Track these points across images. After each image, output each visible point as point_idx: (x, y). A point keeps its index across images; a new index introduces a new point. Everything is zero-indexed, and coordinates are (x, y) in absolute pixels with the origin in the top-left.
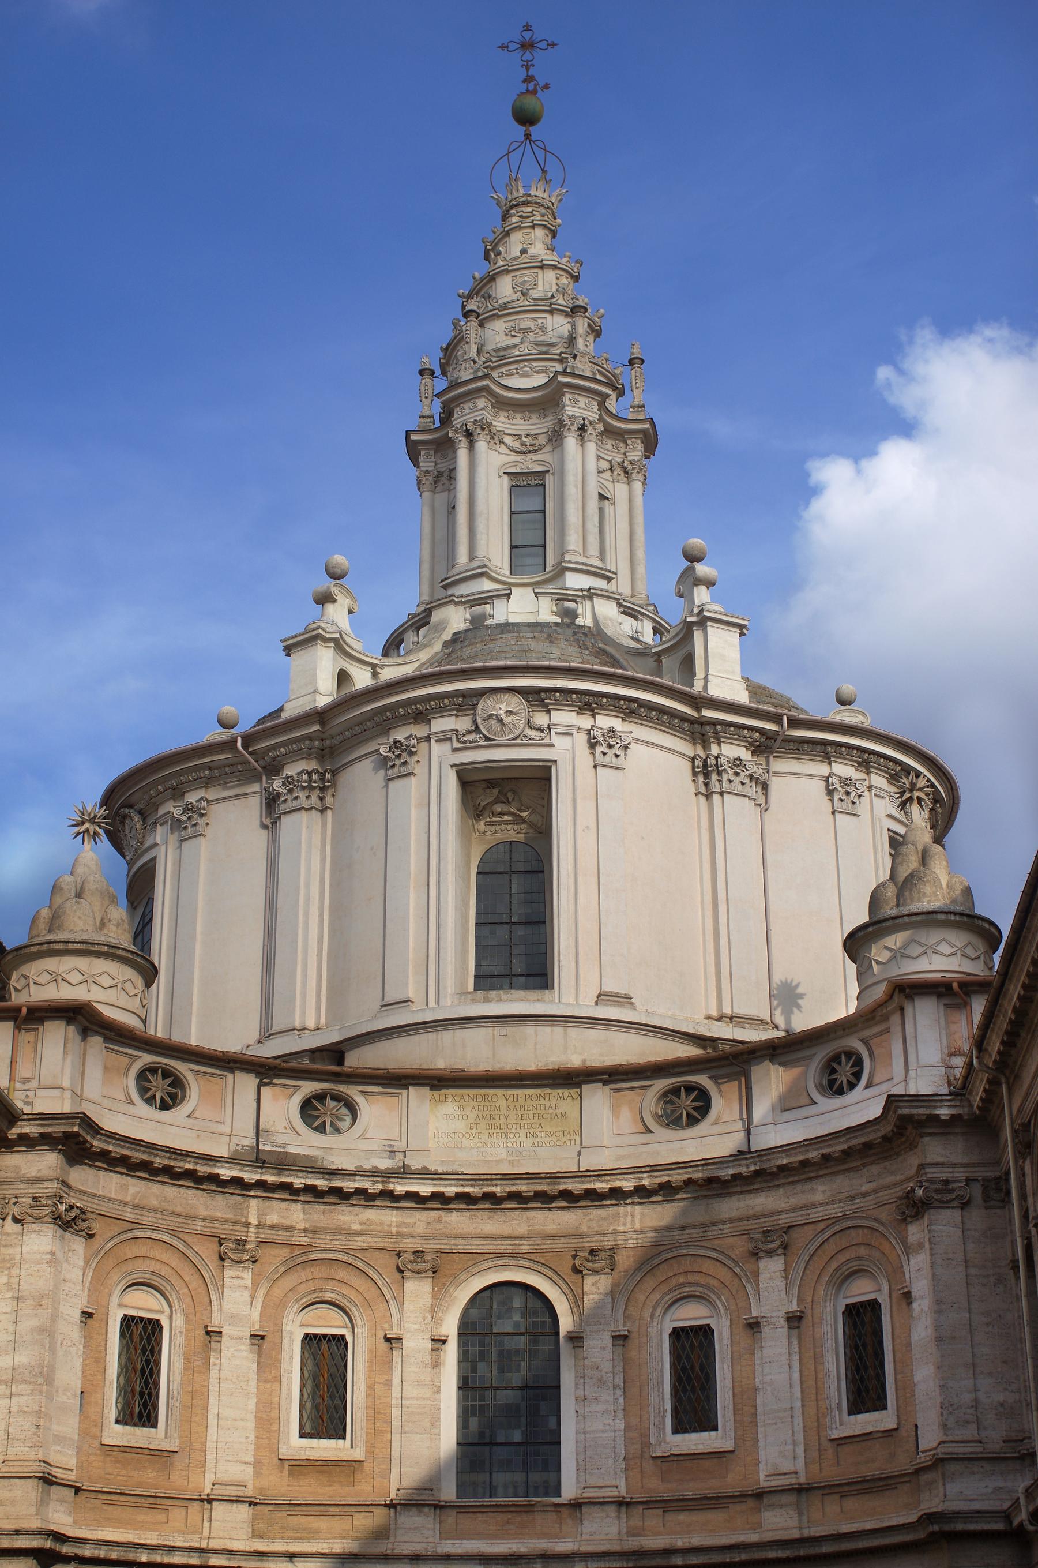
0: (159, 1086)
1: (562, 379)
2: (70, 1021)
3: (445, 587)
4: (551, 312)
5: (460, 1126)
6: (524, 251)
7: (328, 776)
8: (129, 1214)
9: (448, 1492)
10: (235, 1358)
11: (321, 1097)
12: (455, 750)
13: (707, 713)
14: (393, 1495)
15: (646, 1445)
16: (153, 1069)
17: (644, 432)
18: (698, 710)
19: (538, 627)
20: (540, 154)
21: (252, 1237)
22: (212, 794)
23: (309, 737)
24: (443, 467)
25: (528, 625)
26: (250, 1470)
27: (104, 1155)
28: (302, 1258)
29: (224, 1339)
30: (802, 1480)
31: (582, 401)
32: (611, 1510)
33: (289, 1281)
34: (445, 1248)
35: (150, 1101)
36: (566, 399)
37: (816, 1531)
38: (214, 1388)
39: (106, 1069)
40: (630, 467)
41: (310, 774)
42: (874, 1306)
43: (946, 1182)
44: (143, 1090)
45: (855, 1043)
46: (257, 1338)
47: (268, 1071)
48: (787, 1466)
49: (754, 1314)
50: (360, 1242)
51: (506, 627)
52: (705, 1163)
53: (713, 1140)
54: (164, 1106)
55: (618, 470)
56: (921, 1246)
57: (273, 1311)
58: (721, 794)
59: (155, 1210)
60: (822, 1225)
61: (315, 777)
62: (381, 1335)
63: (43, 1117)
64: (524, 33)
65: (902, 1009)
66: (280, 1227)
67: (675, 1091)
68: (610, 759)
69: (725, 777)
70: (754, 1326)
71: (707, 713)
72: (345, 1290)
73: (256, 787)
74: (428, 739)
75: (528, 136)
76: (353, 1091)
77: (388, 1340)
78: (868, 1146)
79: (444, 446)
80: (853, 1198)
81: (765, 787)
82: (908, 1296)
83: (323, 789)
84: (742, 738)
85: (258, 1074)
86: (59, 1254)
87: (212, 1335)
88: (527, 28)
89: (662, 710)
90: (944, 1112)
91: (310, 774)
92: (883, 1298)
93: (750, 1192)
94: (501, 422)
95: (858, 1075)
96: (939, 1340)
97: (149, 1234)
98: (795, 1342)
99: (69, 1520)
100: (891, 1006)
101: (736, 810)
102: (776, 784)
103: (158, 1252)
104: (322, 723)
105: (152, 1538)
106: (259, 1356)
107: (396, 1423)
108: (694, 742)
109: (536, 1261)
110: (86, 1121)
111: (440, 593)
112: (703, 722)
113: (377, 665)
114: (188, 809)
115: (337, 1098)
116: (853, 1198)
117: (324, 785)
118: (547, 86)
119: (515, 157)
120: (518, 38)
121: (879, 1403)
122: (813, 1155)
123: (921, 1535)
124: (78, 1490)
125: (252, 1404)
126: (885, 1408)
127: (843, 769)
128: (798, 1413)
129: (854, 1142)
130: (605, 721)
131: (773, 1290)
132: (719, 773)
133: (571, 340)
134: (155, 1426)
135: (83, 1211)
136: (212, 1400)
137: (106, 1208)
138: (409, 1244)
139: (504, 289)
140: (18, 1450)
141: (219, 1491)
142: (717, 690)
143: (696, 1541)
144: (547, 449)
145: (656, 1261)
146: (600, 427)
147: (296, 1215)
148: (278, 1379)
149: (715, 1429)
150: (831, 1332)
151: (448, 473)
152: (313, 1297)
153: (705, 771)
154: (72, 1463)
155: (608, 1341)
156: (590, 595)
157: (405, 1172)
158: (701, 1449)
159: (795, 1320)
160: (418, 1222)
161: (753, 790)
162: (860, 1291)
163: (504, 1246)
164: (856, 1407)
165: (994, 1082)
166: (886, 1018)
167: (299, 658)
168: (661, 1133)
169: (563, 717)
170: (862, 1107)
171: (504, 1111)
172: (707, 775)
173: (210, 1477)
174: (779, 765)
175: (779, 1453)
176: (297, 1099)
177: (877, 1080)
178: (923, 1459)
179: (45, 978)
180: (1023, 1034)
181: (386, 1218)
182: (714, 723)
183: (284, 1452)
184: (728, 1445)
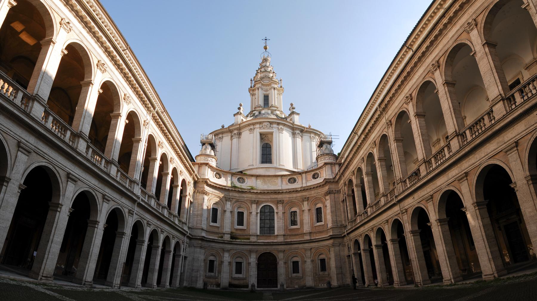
0: (218, 176)
5: (260, 183)
9: (259, 234)
10: (228, 214)
15: (287, 227)
28: (237, 201)
33: (236, 204)
45: (318, 172)
46: (231, 212)
47: (233, 174)
50: (246, 199)
53: (297, 186)
57: (233, 208)
67: (291, 178)
70: (303, 211)
73: (230, 134)
76: (244, 177)
78: (320, 186)
82: (326, 206)
87: (225, 211)
90: (332, 181)
94: (263, 87)
101: (299, 140)
109: (272, 202)
114: (220, 138)
117: (240, 134)
122: (312, 187)
130: (281, 126)
131: (306, 206)
143: (295, 240)
147: (236, 195)
150: (314, 212)
159: (309, 210)
160: (253, 197)
161: (300, 137)
163: (267, 200)
164: (318, 222)
165: (340, 176)
168: (289, 184)
169: (275, 126)
170: (319, 180)
175: (307, 228)
176: (237, 179)
181: (250, 196)
183: (235, 228)
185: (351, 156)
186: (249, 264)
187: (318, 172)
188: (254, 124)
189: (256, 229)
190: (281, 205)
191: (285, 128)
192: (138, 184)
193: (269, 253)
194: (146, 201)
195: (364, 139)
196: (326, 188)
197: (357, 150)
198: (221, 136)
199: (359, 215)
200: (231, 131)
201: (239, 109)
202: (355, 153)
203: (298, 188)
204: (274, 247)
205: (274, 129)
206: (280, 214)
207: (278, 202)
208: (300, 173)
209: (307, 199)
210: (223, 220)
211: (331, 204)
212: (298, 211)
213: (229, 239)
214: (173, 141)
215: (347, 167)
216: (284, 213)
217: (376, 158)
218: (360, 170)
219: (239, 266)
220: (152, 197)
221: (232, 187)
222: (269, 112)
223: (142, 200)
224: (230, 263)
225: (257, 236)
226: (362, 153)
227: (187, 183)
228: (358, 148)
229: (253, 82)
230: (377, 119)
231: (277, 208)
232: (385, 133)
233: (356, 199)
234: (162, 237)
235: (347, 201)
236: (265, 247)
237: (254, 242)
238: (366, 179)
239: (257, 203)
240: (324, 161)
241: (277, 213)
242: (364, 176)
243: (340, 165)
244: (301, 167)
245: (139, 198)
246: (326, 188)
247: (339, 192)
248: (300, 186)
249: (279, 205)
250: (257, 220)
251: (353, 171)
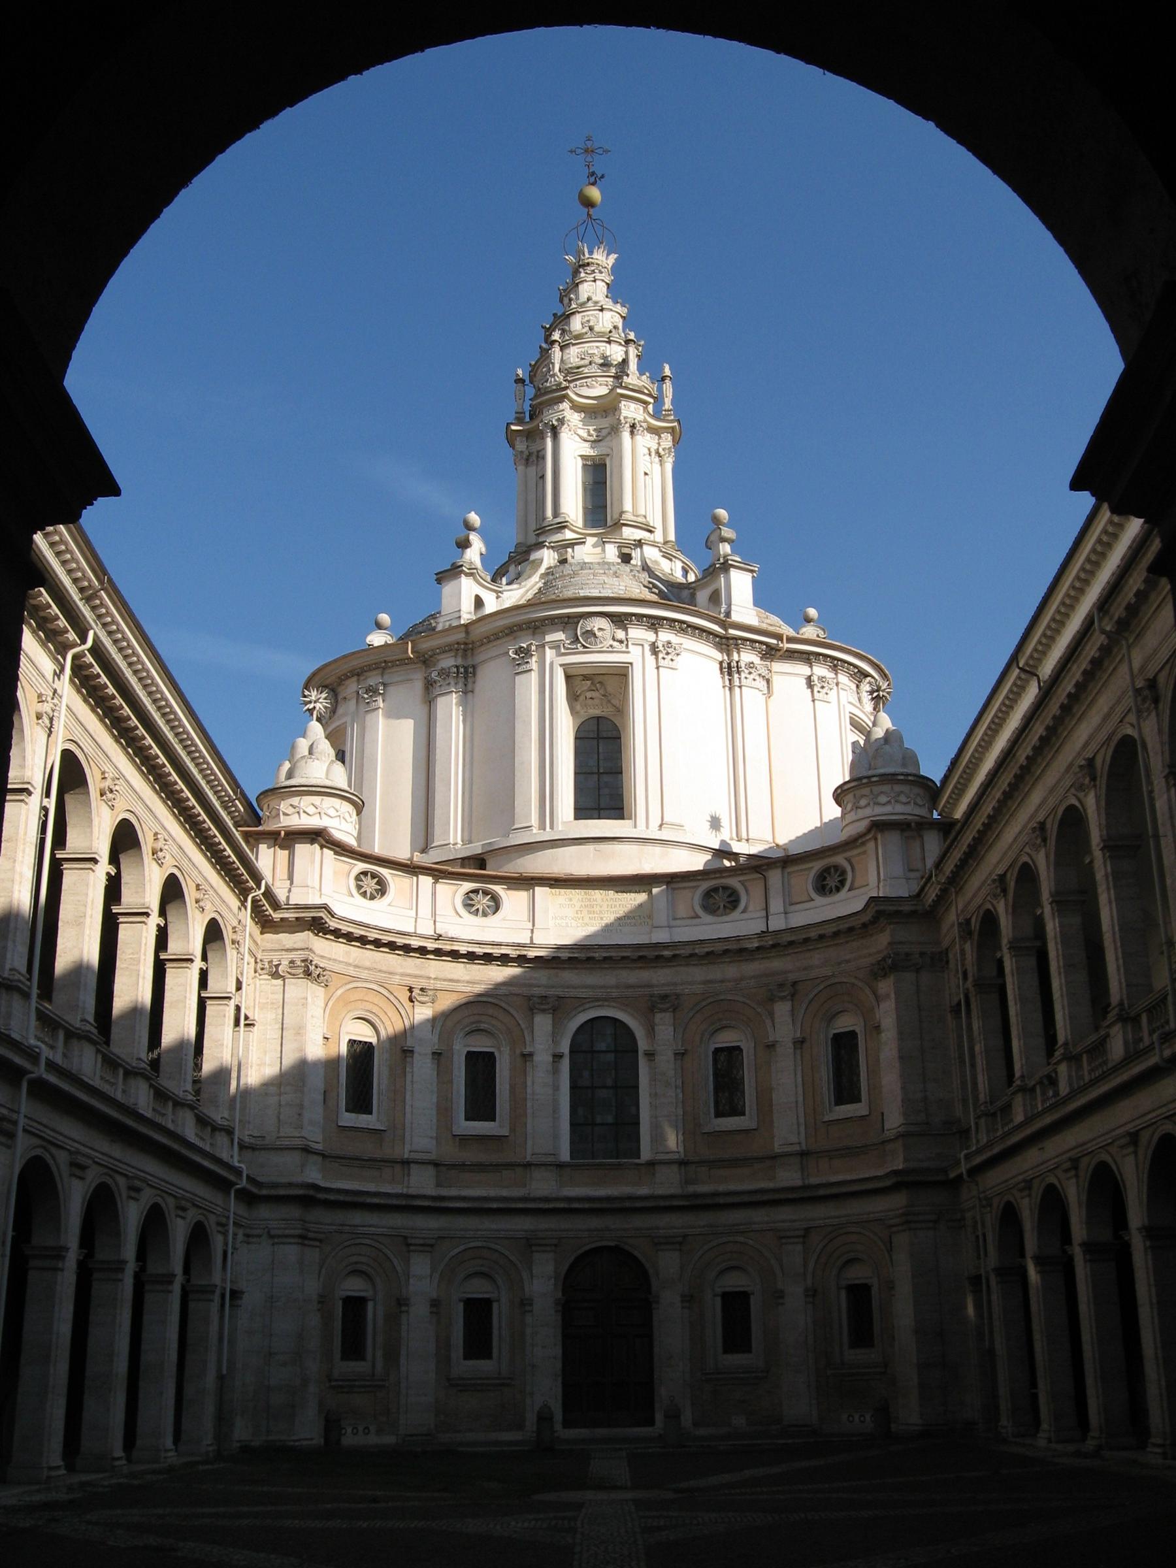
0: (370, 885)
1: (619, 391)
2: (312, 842)
3: (538, 535)
4: (609, 342)
6: (589, 299)
7: (471, 670)
8: (351, 971)
9: (565, 1155)
11: (476, 891)
13: (732, 632)
14: (528, 1159)
16: (365, 873)
17: (673, 428)
18: (726, 630)
19: (604, 564)
21: (431, 984)
22: (387, 678)
24: (534, 448)
25: (599, 563)
26: (434, 1142)
27: (337, 934)
29: (416, 1055)
30: (804, 1148)
31: (633, 406)
32: (675, 1168)
34: (561, 994)
35: (364, 894)
36: (623, 403)
37: (814, 1180)
38: (408, 1087)
39: (335, 872)
40: (662, 453)
41: (457, 667)
42: (853, 1034)
43: (907, 954)
44: (359, 887)
45: (839, 860)
46: (437, 1055)
48: (794, 1139)
49: (771, 1039)
51: (584, 565)
52: (738, 939)
53: (741, 924)
54: (372, 898)
55: (653, 454)
56: (888, 996)
58: (740, 687)
59: (369, 969)
60: (818, 981)
61: (462, 670)
62: (518, 1052)
63: (298, 907)
65: (876, 839)
66: (451, 980)
67: (715, 890)
68: (667, 663)
69: (743, 675)
70: (771, 1047)
71: (732, 632)
72: (494, 1022)
74: (543, 646)
77: (524, 1056)
78: (851, 929)
79: (533, 436)
80: (839, 964)
81: (768, 681)
82: (878, 1028)
84: (754, 648)
85: (434, 876)
86: (309, 999)
89: (702, 630)
90: (906, 908)
91: (457, 667)
92: (858, 1031)
93: (768, 958)
95: (842, 882)
96: (901, 1058)
97: (365, 985)
98: (799, 1057)
99: (320, 1176)
100: (870, 836)
102: (776, 680)
103: (370, 996)
105: (371, 1187)
106: (438, 1065)
107: (529, 1111)
108: (721, 651)
109: (623, 1002)
110: (325, 907)
111: (532, 540)
112: (728, 638)
115: (486, 893)
116: (839, 964)
117: (466, 676)
118: (603, 177)
121: (856, 1099)
122: (813, 934)
123: (888, 1183)
124: (324, 1156)
125: (435, 1100)
126: (860, 1101)
127: (820, 670)
128: (801, 1104)
129: (841, 927)
130: (665, 636)
131: (783, 1024)
132: (739, 672)
133: (625, 362)
134: (371, 1113)
135: (324, 969)
136: (408, 1097)
137: (337, 967)
138: (537, 991)
139: (576, 324)
140: (287, 1131)
141: (414, 1156)
142: (736, 617)
143: (732, 1187)
144: (609, 438)
145: (704, 1003)
146: (644, 425)
148: (451, 1082)
149: (744, 1114)
150: (823, 1053)
152: (474, 1027)
153: (729, 670)
154: (320, 1138)
155: (670, 1054)
156: (639, 544)
157: (532, 945)
158: (734, 1128)
159: (799, 1043)
161: (762, 684)
162: (844, 1023)
164: (840, 1101)
166: (863, 844)
167: (448, 589)
168: (707, 918)
169: (638, 633)
170: (847, 904)
171: (599, 902)
172: (730, 674)
173: (407, 1147)
174: (777, 666)
175: (787, 1132)
177: (856, 885)
178: (889, 1134)
179: (290, 810)
180: (971, 861)
182: (736, 638)
184: (754, 1125)
185: (988, 809)
186: (524, 1304)
187: (839, 860)
188: (538, 627)
189: (556, 1137)
190: (668, 1017)
192: (26, 996)
193: (617, 1247)
194: (58, 1059)
195: (1045, 741)
196: (881, 941)
197: (1014, 787)
198: (373, 680)
199: (1022, 1089)
200: (425, 660)
201: (464, 544)
202: (1008, 796)
203: (748, 938)
204: (638, 1221)
205: (633, 649)
206: (666, 1060)
207: (655, 1004)
208: (759, 865)
209: (792, 990)
210: (398, 1095)
211: (899, 1018)
212: (747, 1047)
213: (431, 1191)
214: (162, 759)
215: (973, 854)
216: (680, 1055)
217: (1096, 837)
218: (1027, 874)
219: (478, 1313)
220: (85, 1037)
221: (438, 938)
222: (612, 552)
223: (51, 1066)
224: (435, 1304)
225: (560, 1166)
226: (1037, 802)
227: (228, 935)
228: (1019, 778)
229: (530, 391)
230: (1097, 663)
231: (651, 1031)
232: (1129, 731)
233: (1013, 1010)
234: (132, 1215)
235: (975, 1013)
236: (595, 1222)
237: (546, 1199)
238: (1052, 927)
239: (555, 1010)
240: (868, 812)
241: (650, 1055)
242: (1047, 910)
243: (946, 827)
244: (760, 835)
245: (34, 1057)
246: (881, 941)
247: (939, 960)
248: (757, 926)
249: (658, 1016)
250: (556, 1088)
251: (1002, 878)
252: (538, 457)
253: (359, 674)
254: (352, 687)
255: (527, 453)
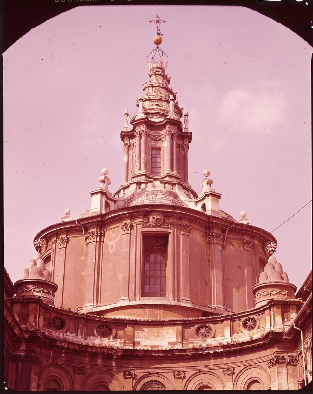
12: (142, 227)
20: (161, 53)
23: (98, 222)
64: (157, 18)
75: (158, 47)
83: (101, 236)
88: (158, 16)
104: (102, 218)
113: (116, 201)
119: (154, 53)
120: (155, 19)
132: (213, 237)
151: (133, 144)
170: (257, 334)
177: (261, 326)
187: (255, 317)
191: (192, 225)
252: (133, 146)
253: (57, 234)
254: (54, 239)
255: (129, 144)
